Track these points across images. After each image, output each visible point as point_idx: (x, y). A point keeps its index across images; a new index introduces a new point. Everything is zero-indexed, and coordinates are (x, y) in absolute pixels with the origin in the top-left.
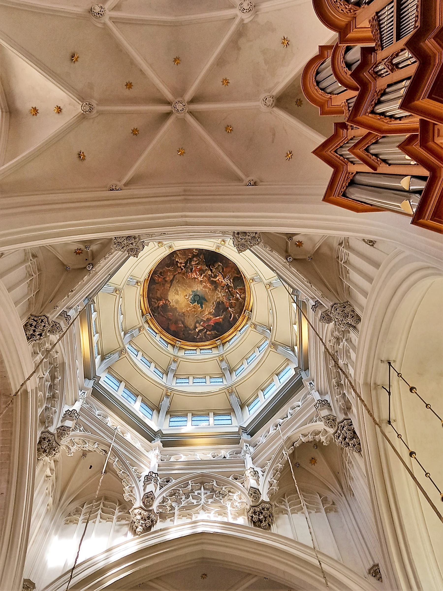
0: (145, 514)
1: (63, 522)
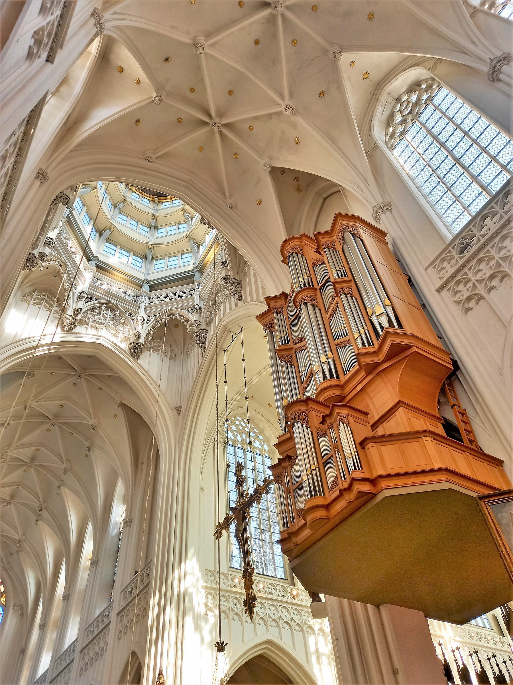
0: (73, 320)
1: (21, 299)
